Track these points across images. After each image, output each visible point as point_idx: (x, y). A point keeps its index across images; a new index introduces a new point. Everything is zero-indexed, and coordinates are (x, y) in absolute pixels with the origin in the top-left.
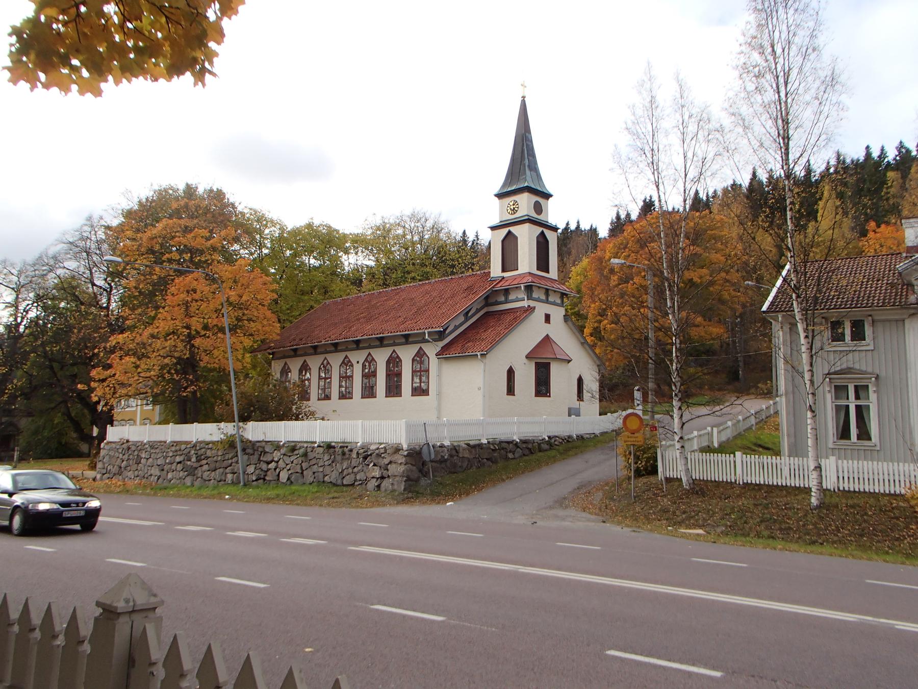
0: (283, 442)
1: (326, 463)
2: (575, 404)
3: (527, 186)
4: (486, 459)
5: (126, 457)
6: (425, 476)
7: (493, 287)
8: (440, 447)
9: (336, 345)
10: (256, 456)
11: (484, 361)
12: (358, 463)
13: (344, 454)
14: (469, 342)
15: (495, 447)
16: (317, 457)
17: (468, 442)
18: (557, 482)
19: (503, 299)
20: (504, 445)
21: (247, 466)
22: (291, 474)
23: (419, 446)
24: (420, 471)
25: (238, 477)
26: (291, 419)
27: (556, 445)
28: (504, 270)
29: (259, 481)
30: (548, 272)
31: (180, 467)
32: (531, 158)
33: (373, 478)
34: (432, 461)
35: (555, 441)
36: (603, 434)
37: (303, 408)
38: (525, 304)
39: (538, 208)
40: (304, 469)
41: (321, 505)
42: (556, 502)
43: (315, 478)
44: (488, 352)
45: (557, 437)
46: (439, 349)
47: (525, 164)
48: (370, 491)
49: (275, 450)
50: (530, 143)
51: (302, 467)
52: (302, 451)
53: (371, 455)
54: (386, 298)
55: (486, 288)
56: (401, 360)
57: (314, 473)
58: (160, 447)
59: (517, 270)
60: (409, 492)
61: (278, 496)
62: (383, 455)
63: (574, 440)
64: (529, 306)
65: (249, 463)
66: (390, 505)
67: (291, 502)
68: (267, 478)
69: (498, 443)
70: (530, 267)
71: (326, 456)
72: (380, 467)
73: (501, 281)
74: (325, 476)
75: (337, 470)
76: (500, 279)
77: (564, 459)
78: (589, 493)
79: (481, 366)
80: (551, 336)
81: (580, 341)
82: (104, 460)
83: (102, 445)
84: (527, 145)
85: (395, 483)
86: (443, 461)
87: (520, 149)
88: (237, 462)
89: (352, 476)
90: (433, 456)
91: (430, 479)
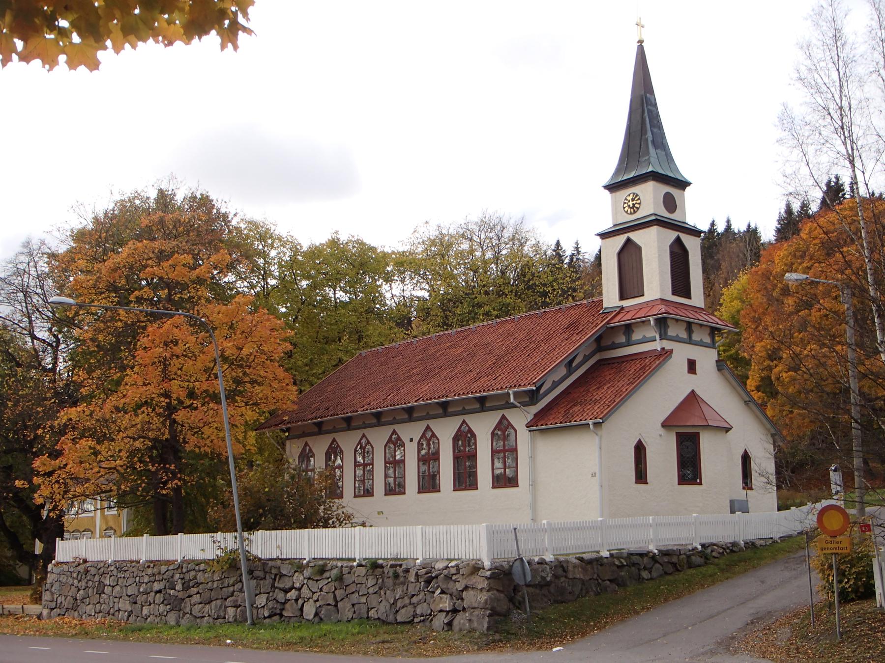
0: (307, 559)
1: (371, 590)
2: (740, 494)
3: (652, 171)
4: (608, 580)
5: (83, 584)
6: (518, 608)
7: (608, 323)
8: (538, 563)
9: (378, 416)
10: (269, 581)
11: (599, 433)
12: (417, 589)
13: (396, 576)
14: (575, 405)
15: (621, 562)
16: (357, 582)
17: (581, 556)
18: (718, 613)
19: (622, 339)
20: (636, 559)
21: (256, 595)
22: (320, 606)
23: (508, 562)
24: (511, 600)
25: (244, 613)
26: (317, 526)
27: (714, 557)
28: (623, 297)
29: (274, 618)
30: (689, 296)
31: (159, 598)
32: (655, 130)
33: (441, 611)
34: (528, 585)
35: (712, 551)
36: (783, 539)
37: (334, 509)
38: (657, 345)
39: (670, 203)
40: (338, 599)
41: (365, 653)
42: (719, 644)
43: (354, 612)
44: (605, 418)
45: (714, 545)
46: (530, 417)
47: (647, 140)
48: (437, 632)
49: (296, 572)
50: (652, 108)
51: (335, 596)
52: (335, 572)
53: (436, 577)
54: (449, 344)
55: (597, 324)
56: (474, 436)
57: (353, 605)
58: (131, 569)
59: (643, 295)
60: (496, 632)
61: (302, 639)
62: (454, 578)
63: (741, 550)
64: (663, 349)
65: (258, 592)
66: (468, 651)
67: (322, 649)
68: (285, 613)
69: (625, 555)
70: (662, 290)
71: (370, 578)
72: (451, 595)
73: (619, 313)
74: (369, 609)
75: (387, 601)
76: (618, 310)
78: (769, 629)
79: (597, 439)
80: (698, 392)
81: (742, 399)
82: (53, 589)
83: (50, 567)
84: (649, 111)
85: (474, 618)
86: (543, 585)
87: (639, 118)
88: (241, 590)
89: (410, 609)
90: (529, 578)
91: (525, 612)
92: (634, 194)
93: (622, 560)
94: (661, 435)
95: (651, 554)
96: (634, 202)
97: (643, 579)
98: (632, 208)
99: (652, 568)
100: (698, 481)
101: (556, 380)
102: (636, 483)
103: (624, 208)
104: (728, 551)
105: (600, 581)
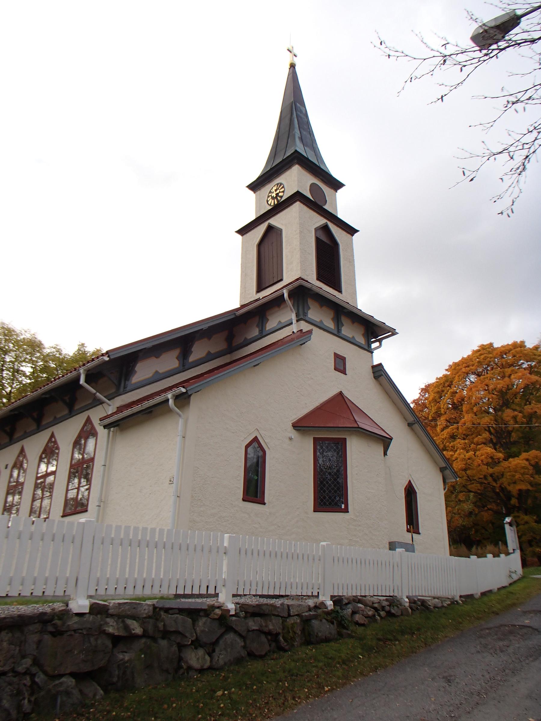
4: (72, 675)
15: (126, 628)
27: (357, 623)
30: (340, 291)
35: (354, 613)
45: (360, 601)
59: (281, 280)
63: (404, 613)
77: (375, 669)
87: (287, 121)
92: (277, 184)
93: (129, 622)
94: (291, 439)
95: (218, 611)
97: (190, 668)
98: (276, 198)
99: (215, 643)
100: (343, 506)
101: (161, 371)
102: (244, 500)
103: (267, 201)
104: (383, 613)
105: (40, 678)
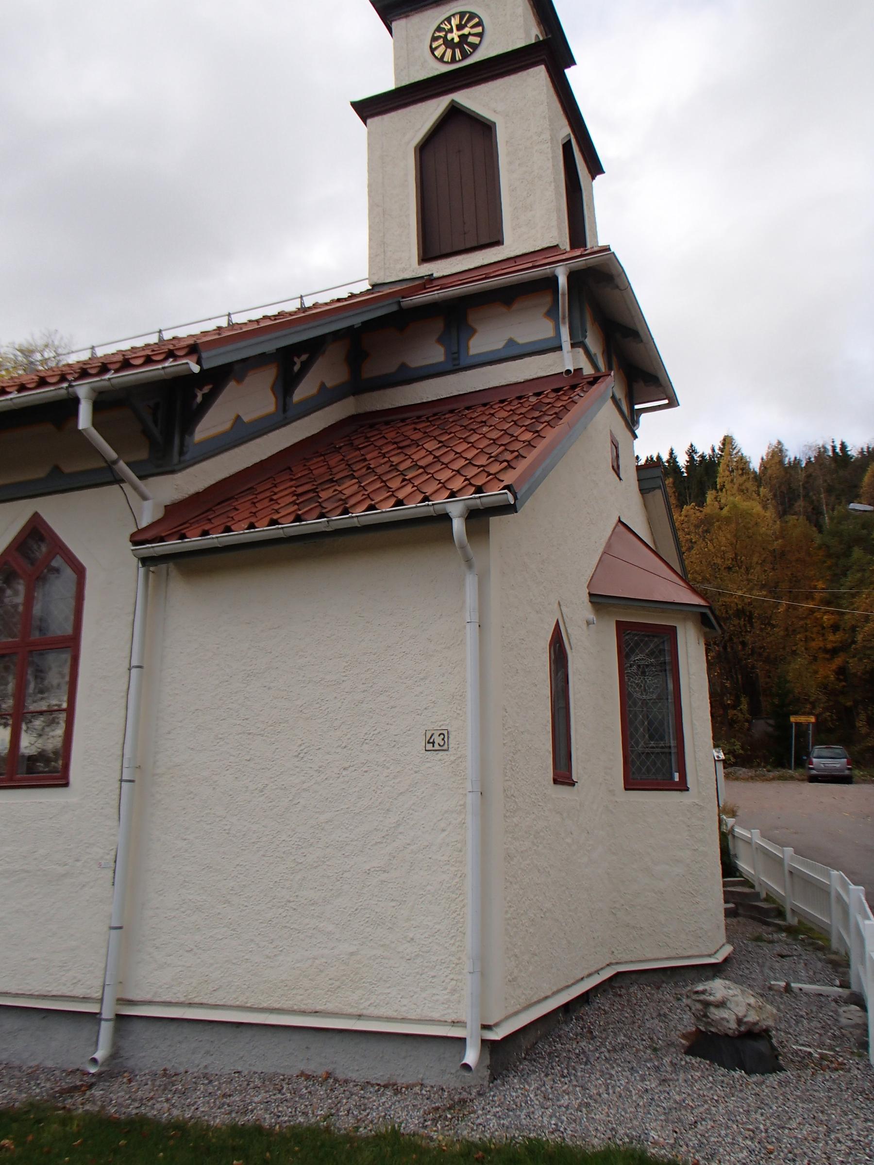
19: (436, 354)
46: (148, 515)
59: (499, 242)
92: (462, 15)
94: (588, 623)
96: (466, 31)
98: (460, 45)
103: (432, 50)
